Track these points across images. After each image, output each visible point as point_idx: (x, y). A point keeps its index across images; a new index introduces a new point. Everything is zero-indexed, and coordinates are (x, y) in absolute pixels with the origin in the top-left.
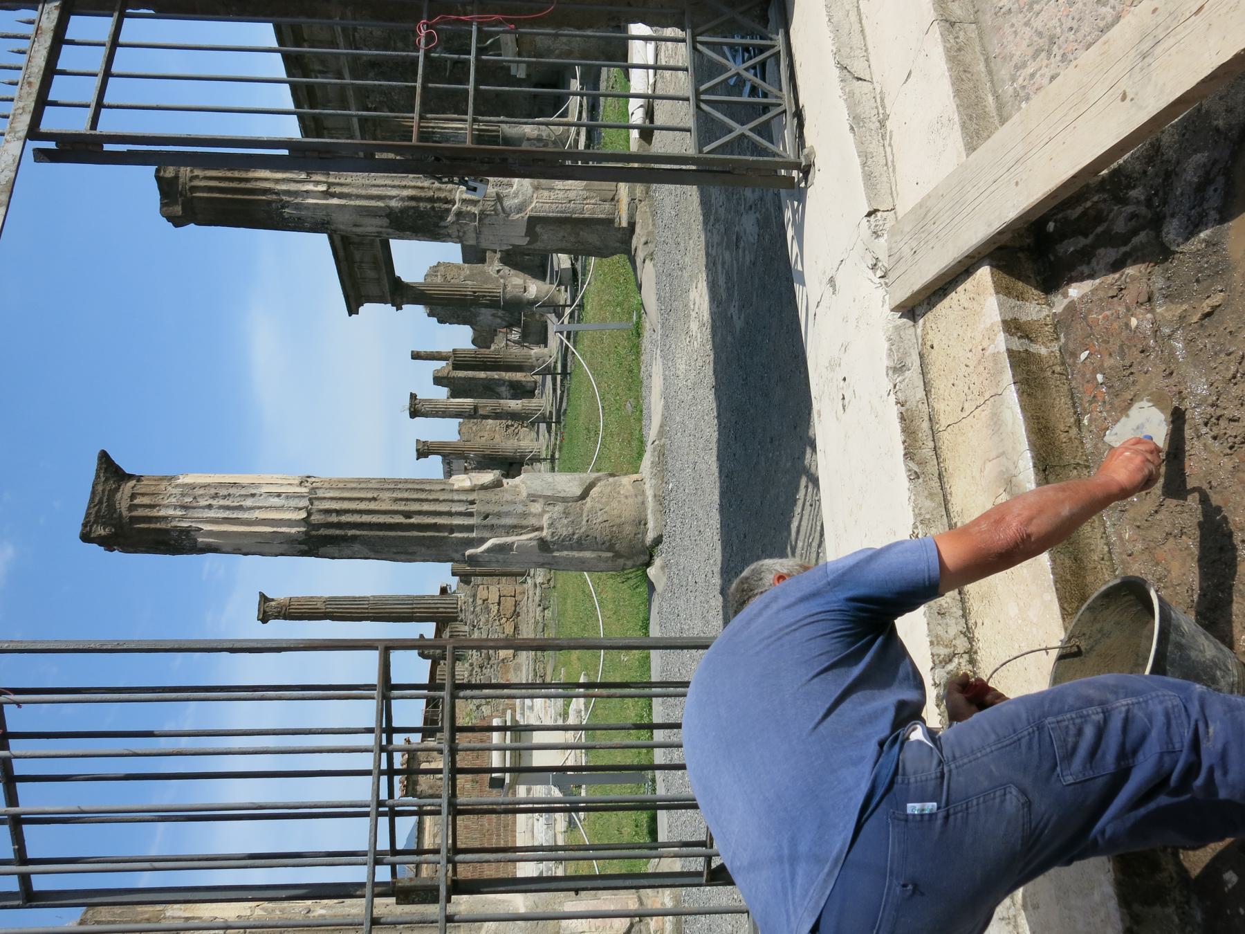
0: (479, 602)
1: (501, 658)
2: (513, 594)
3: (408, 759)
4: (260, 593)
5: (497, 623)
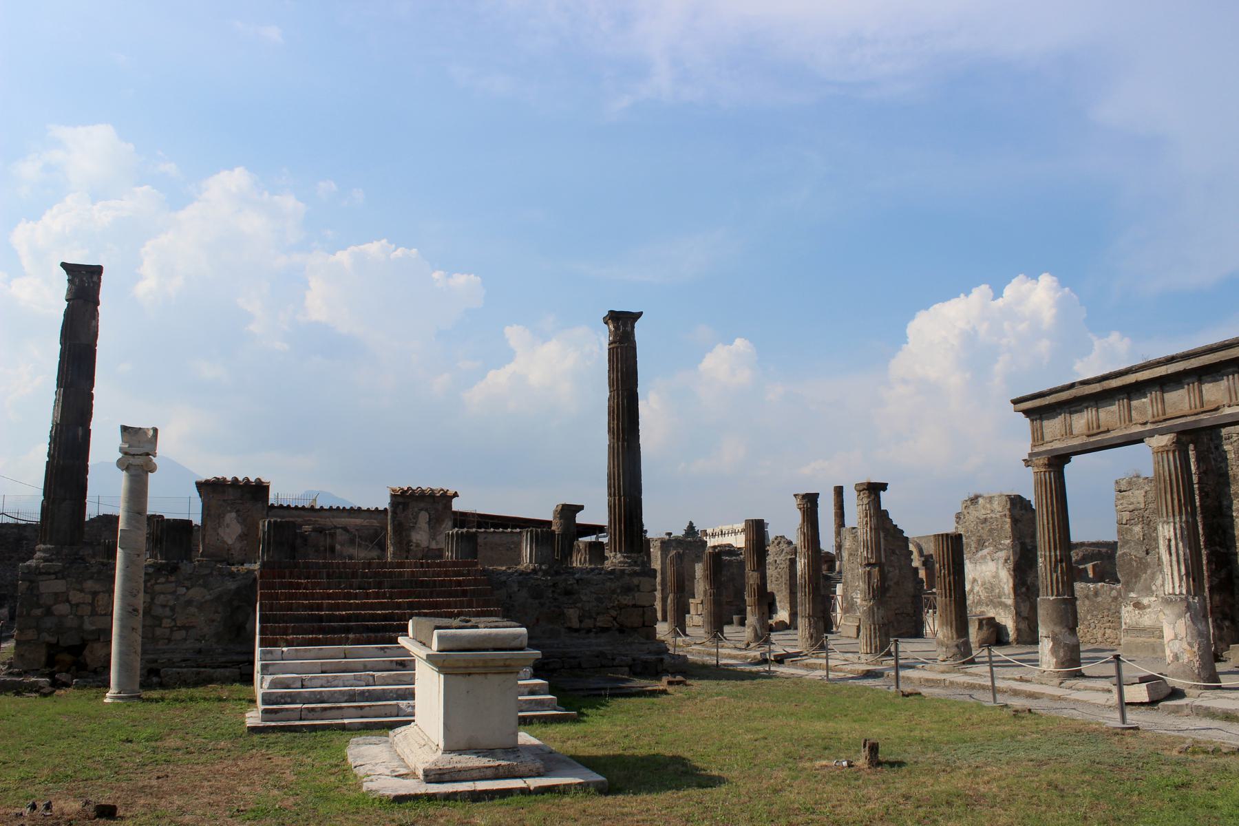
0: (636, 581)
1: (565, 610)
4: (642, 313)
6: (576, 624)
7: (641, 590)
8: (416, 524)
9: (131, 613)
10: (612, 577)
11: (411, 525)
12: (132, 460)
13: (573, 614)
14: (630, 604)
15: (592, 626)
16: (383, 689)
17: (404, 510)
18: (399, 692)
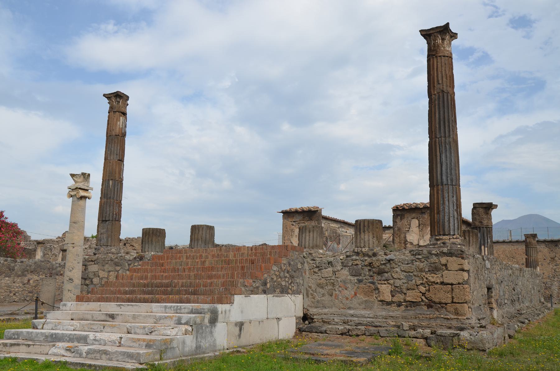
0: (443, 260)
1: (379, 286)
2: (454, 301)
3: (419, 209)
5: (419, 282)
6: (388, 298)
7: (449, 269)
8: (410, 229)
9: (68, 281)
10: (420, 257)
11: (407, 229)
12: (72, 193)
13: (386, 290)
14: (439, 281)
15: (402, 301)
16: (63, 334)
17: (401, 219)
18: (71, 337)
